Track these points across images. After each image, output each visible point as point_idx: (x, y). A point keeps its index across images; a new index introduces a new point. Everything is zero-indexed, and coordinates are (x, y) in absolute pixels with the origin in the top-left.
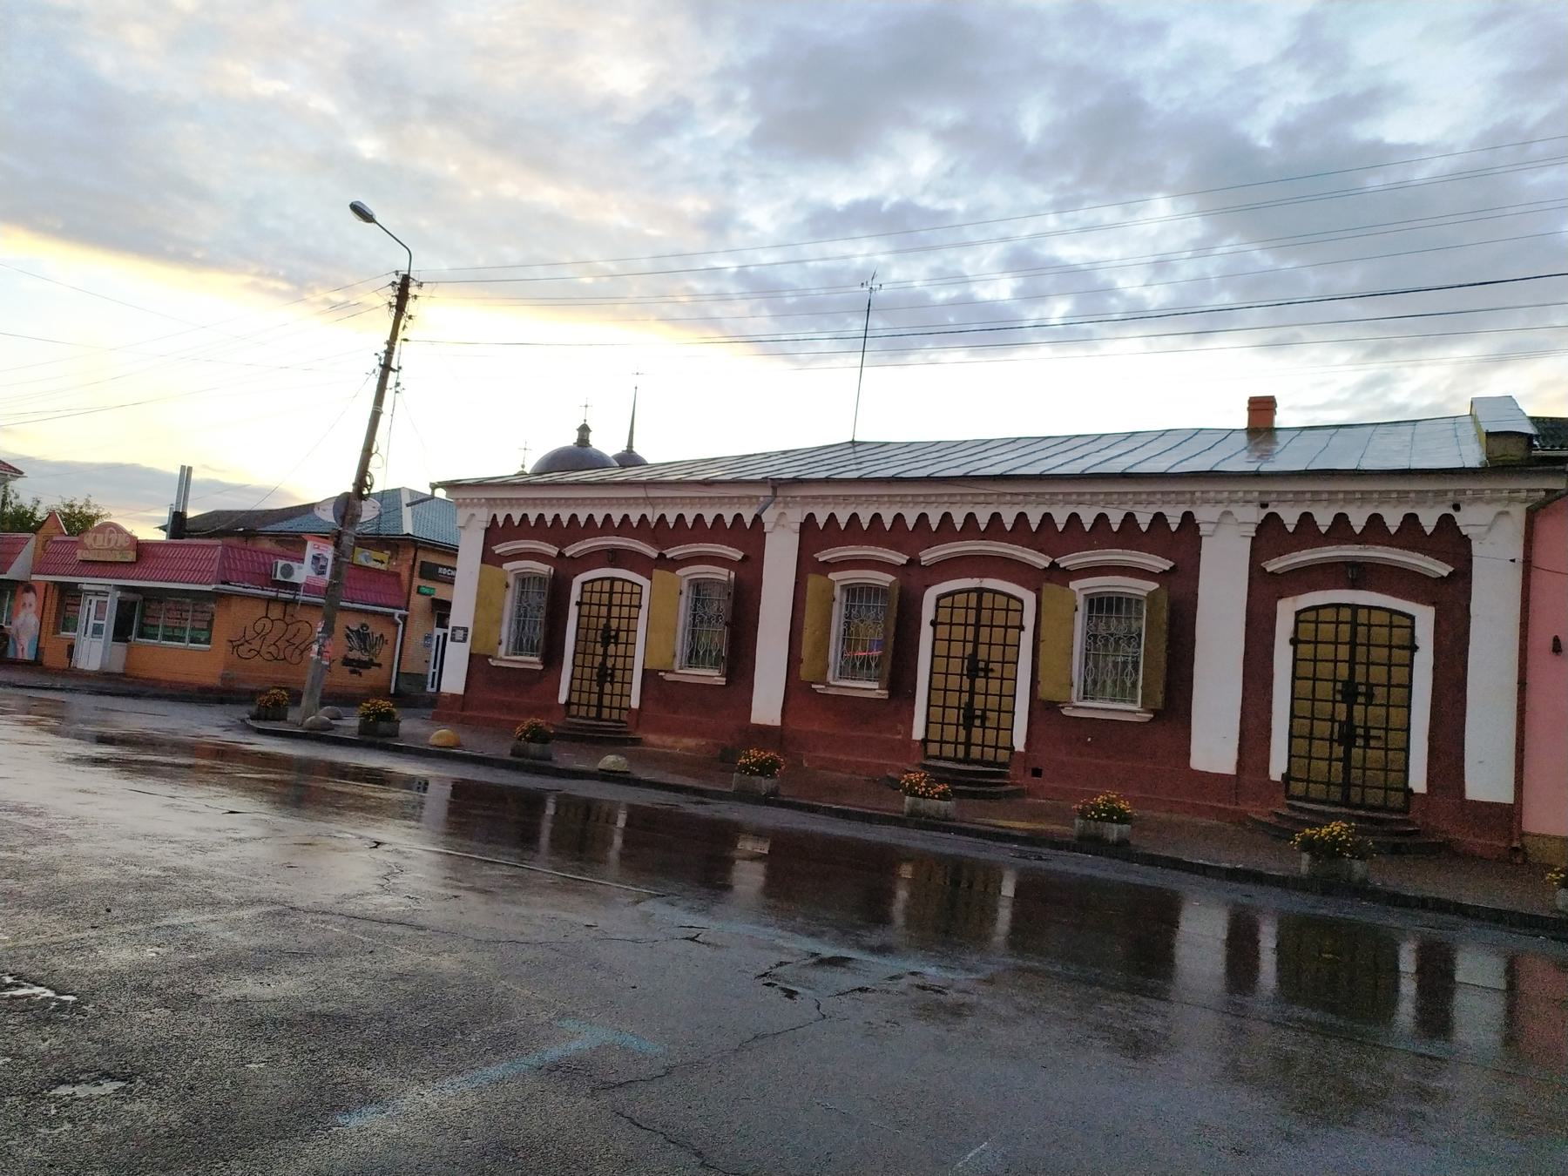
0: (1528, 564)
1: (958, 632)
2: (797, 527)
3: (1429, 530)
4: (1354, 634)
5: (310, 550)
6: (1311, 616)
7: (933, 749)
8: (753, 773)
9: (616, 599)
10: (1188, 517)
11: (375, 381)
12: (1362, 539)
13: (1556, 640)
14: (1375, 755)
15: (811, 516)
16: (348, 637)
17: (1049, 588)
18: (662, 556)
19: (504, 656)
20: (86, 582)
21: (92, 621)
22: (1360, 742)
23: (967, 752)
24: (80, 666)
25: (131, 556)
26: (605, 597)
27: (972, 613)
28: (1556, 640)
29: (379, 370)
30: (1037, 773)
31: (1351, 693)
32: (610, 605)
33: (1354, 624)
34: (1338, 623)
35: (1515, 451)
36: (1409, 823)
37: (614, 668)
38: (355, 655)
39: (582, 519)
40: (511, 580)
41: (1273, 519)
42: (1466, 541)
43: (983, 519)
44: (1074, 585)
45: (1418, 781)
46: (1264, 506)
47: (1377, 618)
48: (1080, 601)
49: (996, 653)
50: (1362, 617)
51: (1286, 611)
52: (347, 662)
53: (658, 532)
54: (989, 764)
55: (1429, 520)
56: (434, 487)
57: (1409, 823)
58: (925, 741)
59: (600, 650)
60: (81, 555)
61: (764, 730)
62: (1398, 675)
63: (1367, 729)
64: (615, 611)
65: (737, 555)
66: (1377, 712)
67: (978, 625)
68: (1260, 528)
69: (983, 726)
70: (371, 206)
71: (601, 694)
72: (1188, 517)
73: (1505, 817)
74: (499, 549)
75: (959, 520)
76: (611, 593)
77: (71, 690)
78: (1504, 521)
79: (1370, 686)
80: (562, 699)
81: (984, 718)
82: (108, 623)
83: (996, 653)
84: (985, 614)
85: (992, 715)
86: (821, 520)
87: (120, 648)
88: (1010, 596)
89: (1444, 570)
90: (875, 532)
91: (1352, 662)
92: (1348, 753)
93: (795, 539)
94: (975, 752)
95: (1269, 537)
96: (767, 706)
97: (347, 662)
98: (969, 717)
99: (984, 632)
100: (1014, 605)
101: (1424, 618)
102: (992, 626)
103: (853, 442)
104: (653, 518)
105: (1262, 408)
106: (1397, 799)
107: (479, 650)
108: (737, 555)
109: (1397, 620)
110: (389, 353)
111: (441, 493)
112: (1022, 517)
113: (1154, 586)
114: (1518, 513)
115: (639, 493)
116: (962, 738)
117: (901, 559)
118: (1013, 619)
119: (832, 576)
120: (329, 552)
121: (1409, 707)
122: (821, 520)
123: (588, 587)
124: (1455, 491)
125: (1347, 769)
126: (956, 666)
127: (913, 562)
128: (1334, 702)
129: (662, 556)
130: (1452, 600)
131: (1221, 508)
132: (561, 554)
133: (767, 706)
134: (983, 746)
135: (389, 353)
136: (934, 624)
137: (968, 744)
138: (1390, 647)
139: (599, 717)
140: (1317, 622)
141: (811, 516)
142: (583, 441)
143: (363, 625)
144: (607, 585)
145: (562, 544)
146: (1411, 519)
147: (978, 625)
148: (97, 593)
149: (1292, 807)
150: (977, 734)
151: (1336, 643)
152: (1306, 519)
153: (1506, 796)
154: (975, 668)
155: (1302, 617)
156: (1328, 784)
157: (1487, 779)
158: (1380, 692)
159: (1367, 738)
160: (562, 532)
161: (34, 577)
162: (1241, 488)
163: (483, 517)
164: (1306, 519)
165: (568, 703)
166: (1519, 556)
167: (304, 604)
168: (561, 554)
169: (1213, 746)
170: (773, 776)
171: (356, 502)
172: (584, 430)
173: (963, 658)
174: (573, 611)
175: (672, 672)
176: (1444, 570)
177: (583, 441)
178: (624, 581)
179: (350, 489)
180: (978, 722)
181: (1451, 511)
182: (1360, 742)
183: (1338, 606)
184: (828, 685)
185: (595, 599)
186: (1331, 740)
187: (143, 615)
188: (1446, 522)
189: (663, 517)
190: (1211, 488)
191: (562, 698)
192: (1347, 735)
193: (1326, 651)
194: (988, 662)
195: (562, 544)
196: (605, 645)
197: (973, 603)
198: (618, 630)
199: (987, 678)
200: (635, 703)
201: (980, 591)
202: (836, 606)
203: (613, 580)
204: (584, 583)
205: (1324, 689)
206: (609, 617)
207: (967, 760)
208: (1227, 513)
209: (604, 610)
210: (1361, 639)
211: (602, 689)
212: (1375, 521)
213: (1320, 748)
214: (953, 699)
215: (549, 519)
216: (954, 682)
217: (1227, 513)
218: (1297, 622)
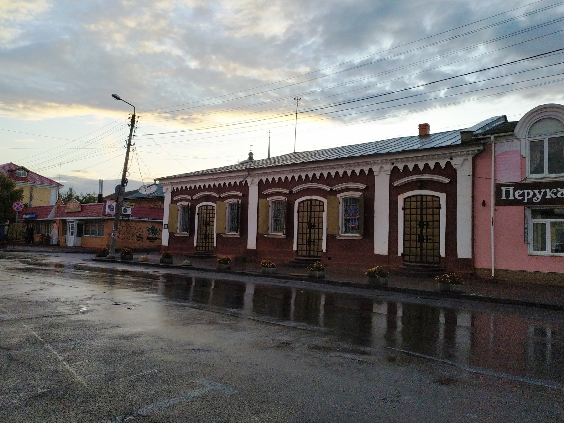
0: (474, 176)
1: (305, 214)
3: (443, 168)
4: (422, 204)
5: (108, 204)
6: (409, 200)
7: (300, 253)
8: (221, 263)
10: (370, 170)
11: (126, 150)
12: (423, 172)
13: (484, 201)
14: (430, 245)
16: (148, 230)
17: (332, 197)
18: (220, 197)
19: (180, 233)
20: (68, 219)
21: (71, 231)
22: (425, 241)
24: (68, 245)
25: (80, 210)
28: (484, 201)
29: (127, 146)
30: (330, 259)
31: (421, 224)
33: (422, 202)
34: (417, 201)
35: (468, 138)
36: (439, 267)
38: (151, 236)
39: (198, 187)
40: (180, 208)
41: (396, 168)
42: (455, 170)
44: (338, 196)
45: (443, 253)
46: (393, 164)
47: (429, 199)
48: (341, 200)
49: (317, 221)
50: (424, 199)
51: (401, 199)
52: (148, 238)
53: (219, 189)
54: (316, 257)
55: (443, 164)
56: (155, 180)
57: (439, 267)
58: (297, 251)
59: (205, 228)
60: (66, 210)
61: (251, 250)
62: (436, 217)
63: (427, 236)
66: (430, 230)
67: (311, 212)
69: (314, 245)
70: (119, 95)
71: (206, 243)
72: (370, 170)
73: (469, 263)
74: (175, 198)
76: (207, 210)
77: (57, 252)
78: (466, 162)
79: (427, 222)
80: (195, 245)
81: (314, 242)
82: (75, 231)
83: (317, 221)
84: (313, 207)
86: (264, 181)
87: (79, 239)
88: (320, 201)
89: (447, 181)
90: (279, 184)
91: (422, 214)
94: (312, 253)
95: (395, 174)
96: (252, 243)
97: (148, 238)
98: (310, 242)
99: (313, 213)
100: (321, 204)
101: (443, 197)
102: (315, 211)
103: (295, 153)
104: (217, 185)
105: (424, 128)
107: (171, 231)
108: (241, 194)
109: (435, 199)
110: (130, 140)
111: (157, 182)
112: (314, 175)
114: (470, 158)
115: (211, 177)
117: (287, 192)
119: (268, 199)
120: (114, 204)
121: (439, 228)
122: (264, 181)
124: (450, 153)
125: (421, 250)
126: (305, 225)
127: (291, 192)
128: (417, 228)
129: (220, 197)
131: (380, 166)
132: (192, 199)
133: (252, 243)
134: (302, 251)
135: (130, 140)
136: (298, 212)
137: (310, 251)
138: (433, 208)
139: (205, 250)
140: (411, 202)
141: (261, 180)
142: (251, 158)
143: (153, 226)
144: (205, 207)
145: (192, 195)
146: (437, 164)
148: (71, 222)
149: (404, 265)
150: (312, 247)
151: (417, 208)
152: (406, 167)
153: (469, 256)
154: (311, 226)
155: (406, 200)
156: (416, 256)
157: (464, 251)
158: (431, 223)
159: (427, 239)
160: (191, 191)
161: (55, 218)
162: (384, 158)
163: (170, 188)
164: (406, 167)
165: (197, 246)
166: (471, 174)
167: (132, 221)
168: (192, 199)
169: (381, 247)
170: (227, 263)
171: (122, 188)
172: (251, 154)
174: (197, 216)
175: (225, 234)
176: (447, 181)
177: (251, 158)
179: (120, 184)
180: (312, 243)
181: (449, 160)
182: (425, 241)
183: (417, 196)
184: (269, 235)
186: (416, 241)
187: (85, 228)
188: (448, 164)
190: (376, 159)
191: (195, 245)
192: (421, 239)
193: (414, 211)
194: (314, 223)
195: (192, 195)
196: (206, 227)
197: (309, 204)
198: (209, 222)
200: (215, 245)
201: (311, 200)
202: (270, 210)
203: (207, 205)
205: (414, 224)
206: (207, 218)
207: (310, 256)
208: (382, 167)
209: (205, 215)
210: (424, 206)
211: (206, 241)
212: (426, 165)
213: (413, 244)
215: (188, 187)
217: (382, 167)
218: (405, 202)
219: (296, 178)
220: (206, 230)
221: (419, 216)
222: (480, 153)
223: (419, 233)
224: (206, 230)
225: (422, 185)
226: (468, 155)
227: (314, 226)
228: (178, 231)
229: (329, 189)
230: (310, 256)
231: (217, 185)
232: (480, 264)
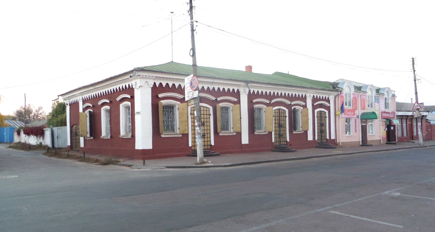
95: (315, 100)
104: (211, 88)
114: (334, 96)
117: (268, 102)
129: (216, 100)
137: (280, 142)
147: (280, 116)
150: (281, 139)
198: (204, 122)
222: (338, 95)
231: (211, 88)
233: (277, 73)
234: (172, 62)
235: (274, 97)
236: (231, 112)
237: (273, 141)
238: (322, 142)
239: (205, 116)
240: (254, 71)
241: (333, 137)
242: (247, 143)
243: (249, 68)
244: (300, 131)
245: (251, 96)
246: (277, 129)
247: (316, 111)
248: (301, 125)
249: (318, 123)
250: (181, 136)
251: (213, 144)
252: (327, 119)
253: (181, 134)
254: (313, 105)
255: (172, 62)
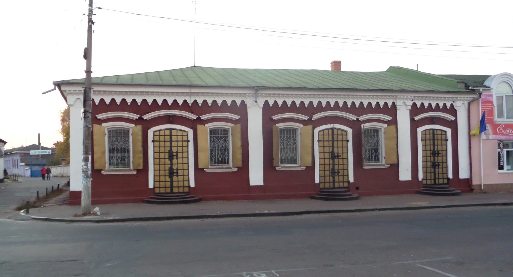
1: (326, 144)
2: (262, 106)
9: (174, 138)
15: (267, 102)
23: (334, 185)
26: (168, 138)
27: (331, 137)
32: (171, 141)
33: (433, 134)
37: (177, 170)
41: (415, 105)
42: (456, 110)
43: (332, 104)
47: (439, 132)
51: (420, 130)
64: (174, 144)
65: (236, 117)
66: (440, 158)
68: (412, 107)
69: (339, 176)
71: (172, 181)
72: (393, 103)
73: (468, 182)
74: (100, 116)
75: (324, 104)
81: (338, 173)
83: (340, 150)
85: (341, 172)
86: (271, 103)
88: (342, 130)
89: (453, 118)
91: (434, 145)
92: (435, 170)
93: (261, 110)
94: (337, 185)
95: (415, 110)
98: (333, 173)
99: (336, 143)
100: (344, 133)
101: (449, 131)
102: (338, 141)
104: (190, 101)
106: (446, 181)
108: (236, 117)
113: (385, 126)
114: (466, 103)
116: (331, 181)
117: (306, 118)
118: (344, 138)
122: (271, 103)
123: (157, 133)
130: (454, 125)
131: (402, 101)
137: (334, 182)
141: (267, 102)
146: (445, 105)
147: (333, 141)
154: (334, 156)
173: (329, 153)
176: (453, 118)
178: (177, 130)
180: (336, 174)
183: (430, 129)
185: (162, 138)
188: (452, 105)
189: (195, 101)
197: (330, 133)
198: (177, 152)
199: (338, 159)
203: (171, 130)
204: (154, 132)
206: (171, 147)
209: (168, 144)
214: (327, 167)
216: (327, 161)
219: (315, 104)
220: (171, 164)
221: (432, 147)
222: (474, 100)
223: (432, 160)
224: (171, 164)
225: (432, 120)
226: (466, 100)
227: (338, 156)
228: (107, 165)
229: (355, 119)
230: (334, 188)
232: (475, 182)
233: (393, 70)
234: (195, 66)
235: (320, 108)
236: (299, 136)
237: (317, 181)
238: (435, 184)
239: (180, 144)
240: (344, 68)
241: (464, 174)
242: (261, 183)
243: (337, 65)
244: (383, 165)
245: (269, 111)
246: (327, 161)
247: (420, 130)
248: (384, 155)
249: (424, 150)
250: (135, 173)
251: (192, 184)
252: (191, 145)
253: (135, 170)
254: (412, 120)
255: (195, 66)
